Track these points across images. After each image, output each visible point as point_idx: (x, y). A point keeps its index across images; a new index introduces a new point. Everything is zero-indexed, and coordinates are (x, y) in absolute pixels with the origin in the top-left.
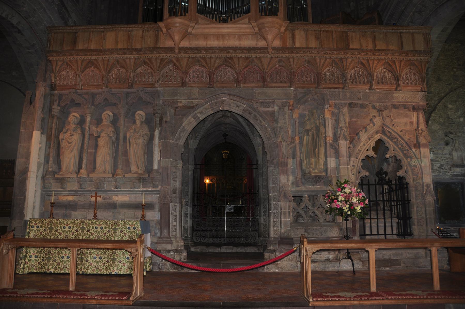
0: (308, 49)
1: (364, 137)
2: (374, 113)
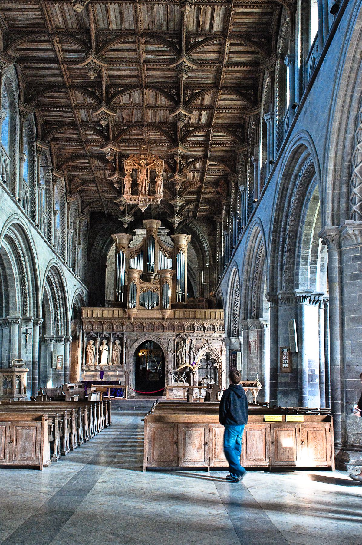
1: (201, 351)
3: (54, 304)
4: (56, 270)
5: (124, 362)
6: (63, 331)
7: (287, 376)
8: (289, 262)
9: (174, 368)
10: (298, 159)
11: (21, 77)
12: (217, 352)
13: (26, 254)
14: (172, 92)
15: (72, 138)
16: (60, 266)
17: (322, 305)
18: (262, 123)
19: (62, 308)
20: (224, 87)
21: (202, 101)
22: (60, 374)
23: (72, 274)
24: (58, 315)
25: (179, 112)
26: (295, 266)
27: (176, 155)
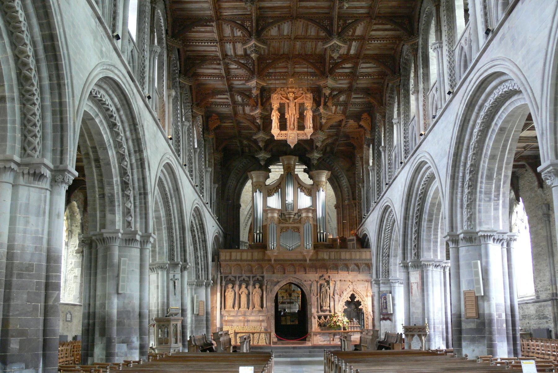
0: (323, 260)
1: (345, 293)
2: (350, 283)
3: (194, 247)
4: (197, 210)
5: (265, 306)
6: (203, 275)
7: (473, 322)
8: (470, 199)
9: (318, 312)
10: (485, 88)
11: (169, 12)
12: (362, 293)
13: (173, 195)
14: (324, 22)
15: (213, 73)
16: (202, 206)
17: (505, 244)
18: (420, 53)
19: (202, 251)
20: (379, 17)
21: (354, 32)
22: (202, 320)
23: (211, 214)
24: (198, 258)
25: (333, 43)
26: (477, 203)
27: (325, 87)
